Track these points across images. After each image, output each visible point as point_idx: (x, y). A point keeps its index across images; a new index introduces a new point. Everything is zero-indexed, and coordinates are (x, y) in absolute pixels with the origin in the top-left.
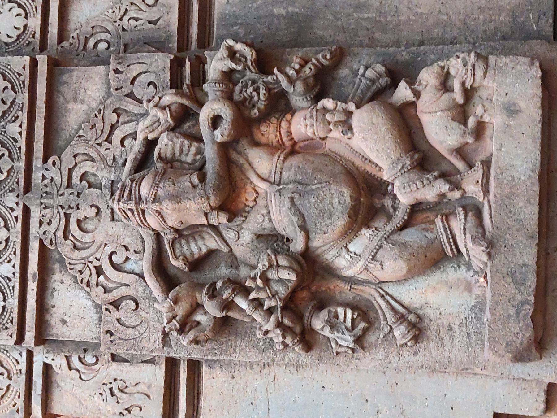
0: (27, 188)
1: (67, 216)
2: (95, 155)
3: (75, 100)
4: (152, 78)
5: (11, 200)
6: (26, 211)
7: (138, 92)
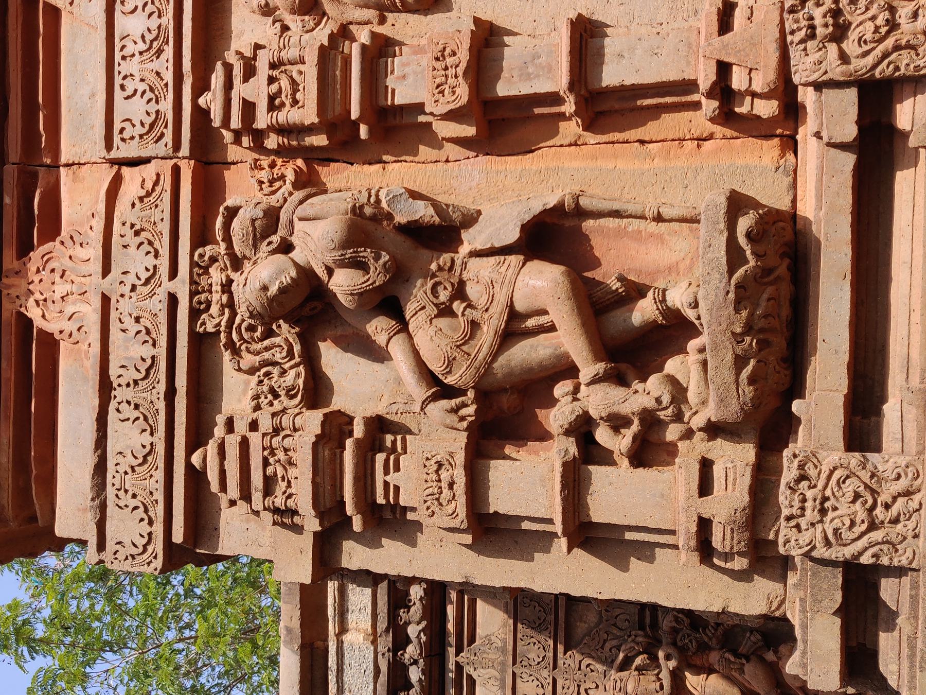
0: (555, 667)
1: (579, 686)
2: (594, 655)
3: (581, 621)
4: (628, 617)
5: (545, 673)
6: (555, 681)
7: (619, 624)
